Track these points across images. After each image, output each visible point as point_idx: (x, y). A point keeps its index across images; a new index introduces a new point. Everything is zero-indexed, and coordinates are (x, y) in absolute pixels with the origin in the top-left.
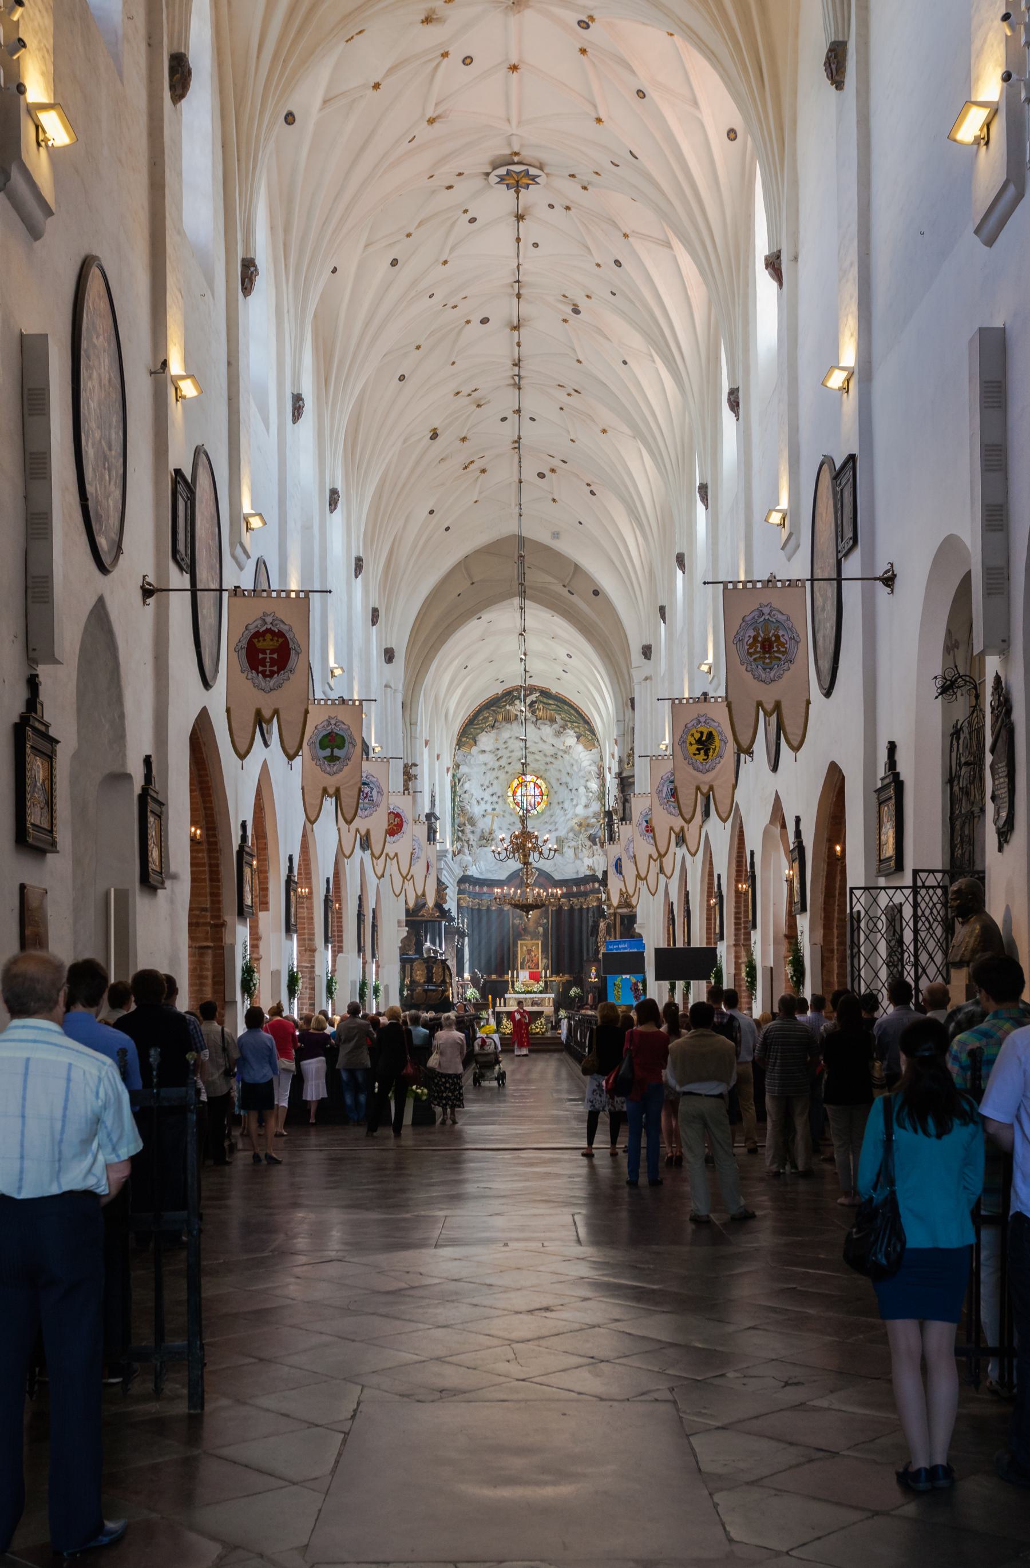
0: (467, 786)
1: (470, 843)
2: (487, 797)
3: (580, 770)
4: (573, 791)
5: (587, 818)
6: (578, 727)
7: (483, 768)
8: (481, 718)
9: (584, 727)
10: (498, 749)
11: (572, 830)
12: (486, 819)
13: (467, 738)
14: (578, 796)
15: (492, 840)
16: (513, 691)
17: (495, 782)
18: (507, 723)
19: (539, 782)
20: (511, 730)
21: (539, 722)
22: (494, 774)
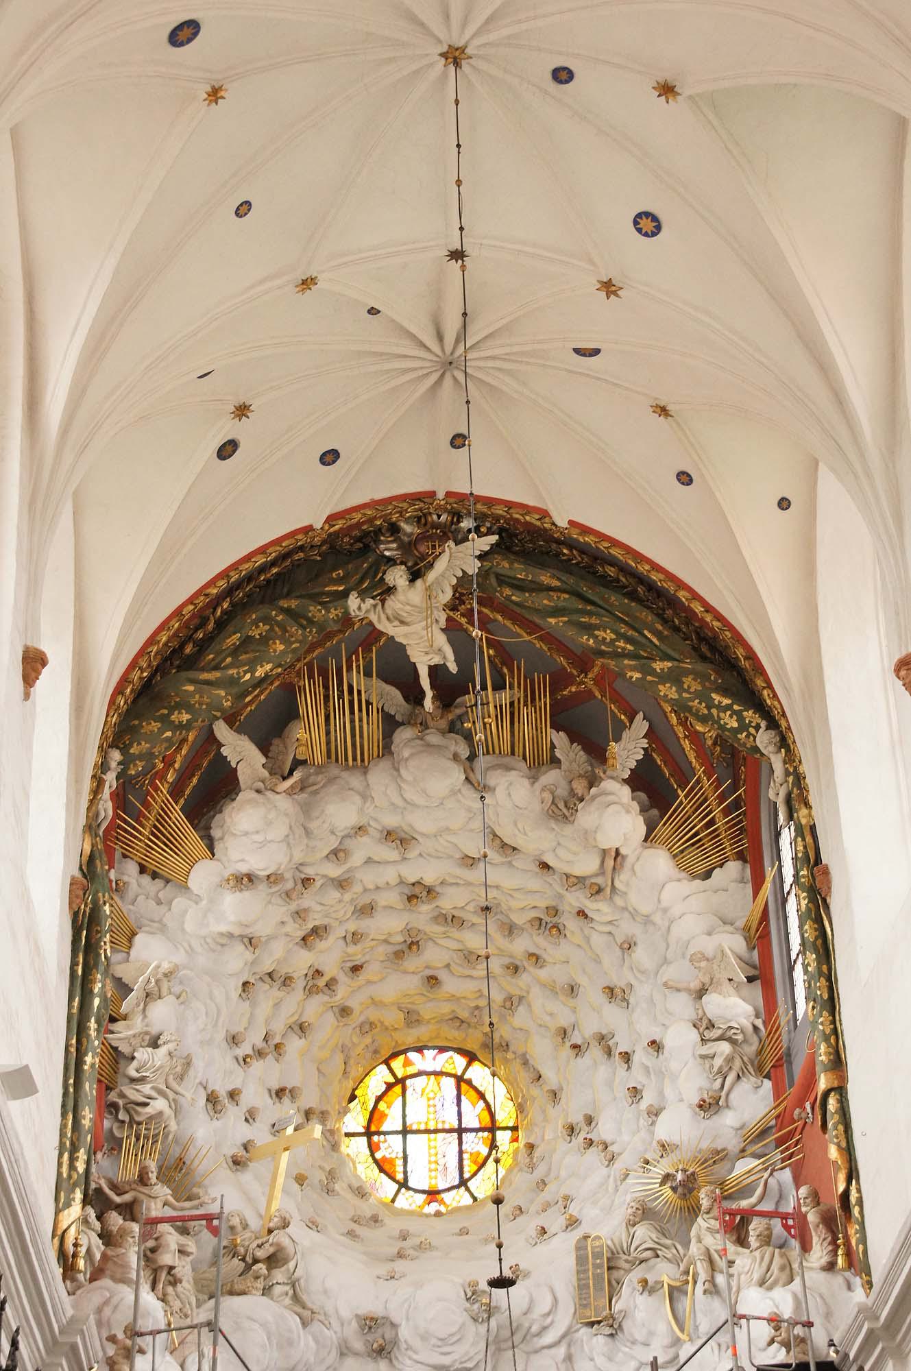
0: (161, 1014)
1: (166, 1259)
2: (254, 1095)
3: (665, 961)
4: (641, 1056)
5: (718, 1156)
6: (674, 678)
7: (237, 961)
8: (235, 639)
9: (703, 677)
10: (306, 882)
11: (644, 1213)
12: (246, 1177)
13: (164, 720)
14: (661, 1074)
15: (275, 1260)
16: (378, 531)
17: (295, 1045)
18: (347, 768)
19: (479, 1074)
20: (365, 797)
21: (482, 762)
22: (293, 1004)
